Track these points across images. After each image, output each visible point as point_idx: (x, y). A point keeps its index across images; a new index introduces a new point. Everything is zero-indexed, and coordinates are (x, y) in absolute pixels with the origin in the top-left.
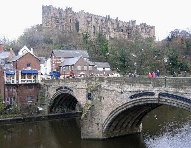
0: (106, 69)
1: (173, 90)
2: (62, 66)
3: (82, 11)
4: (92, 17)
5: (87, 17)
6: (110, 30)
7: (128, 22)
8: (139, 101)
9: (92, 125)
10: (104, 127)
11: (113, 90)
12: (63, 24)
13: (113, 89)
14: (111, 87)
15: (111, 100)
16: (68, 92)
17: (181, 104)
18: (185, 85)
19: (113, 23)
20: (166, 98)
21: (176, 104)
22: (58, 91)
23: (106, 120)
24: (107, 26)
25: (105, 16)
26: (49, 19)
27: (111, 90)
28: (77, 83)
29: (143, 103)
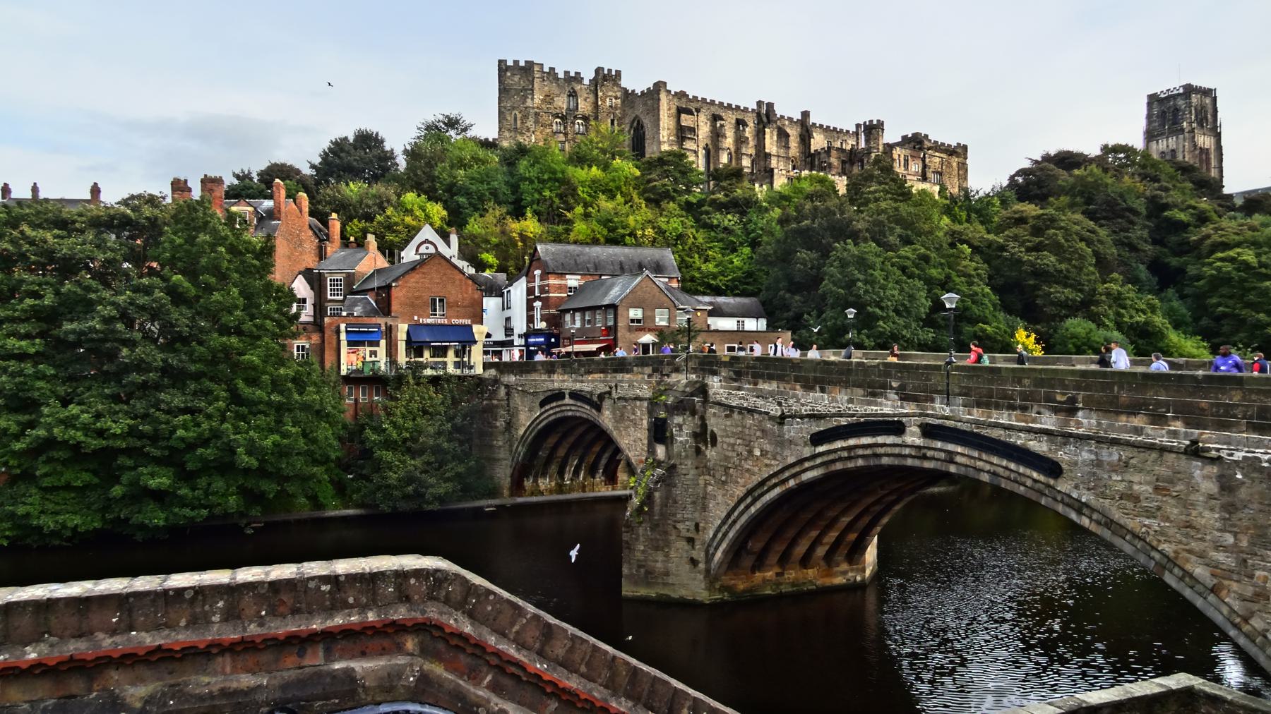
1: (977, 414)
2: (567, 311)
3: (659, 86)
4: (698, 110)
5: (680, 111)
6: (773, 162)
7: (853, 129)
8: (845, 454)
9: (668, 544)
10: (714, 555)
11: (746, 409)
13: (751, 406)
14: (742, 396)
15: (740, 449)
16: (586, 411)
17: (1007, 473)
18: (1025, 397)
19: (788, 136)
20: (951, 447)
21: (988, 472)
22: (547, 407)
23: (720, 527)
24: (760, 145)
26: (525, 117)
27: (742, 410)
28: (620, 376)
29: (860, 462)
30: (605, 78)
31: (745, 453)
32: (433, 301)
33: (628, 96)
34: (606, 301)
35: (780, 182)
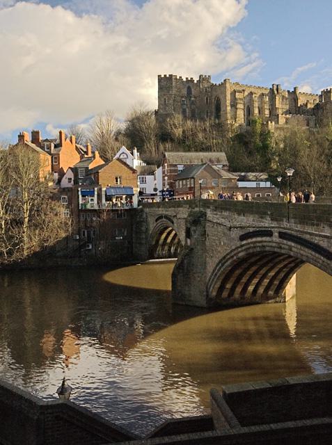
0: (262, 184)
1: (299, 227)
12: (193, 107)
23: (211, 276)
29: (258, 249)
31: (218, 244)
32: (117, 179)
33: (213, 86)
34: (191, 176)
35: (282, 120)
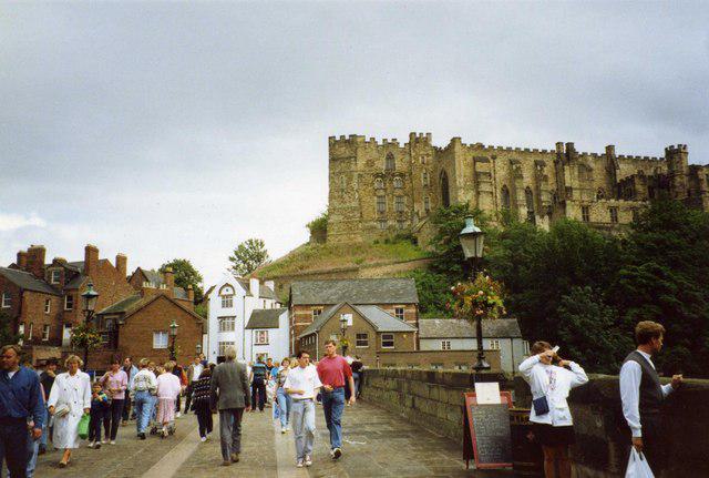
3: (454, 140)
4: (494, 158)
5: (475, 160)
19: (591, 170)
25: (551, 147)
26: (350, 179)
30: (418, 141)
33: (437, 151)
